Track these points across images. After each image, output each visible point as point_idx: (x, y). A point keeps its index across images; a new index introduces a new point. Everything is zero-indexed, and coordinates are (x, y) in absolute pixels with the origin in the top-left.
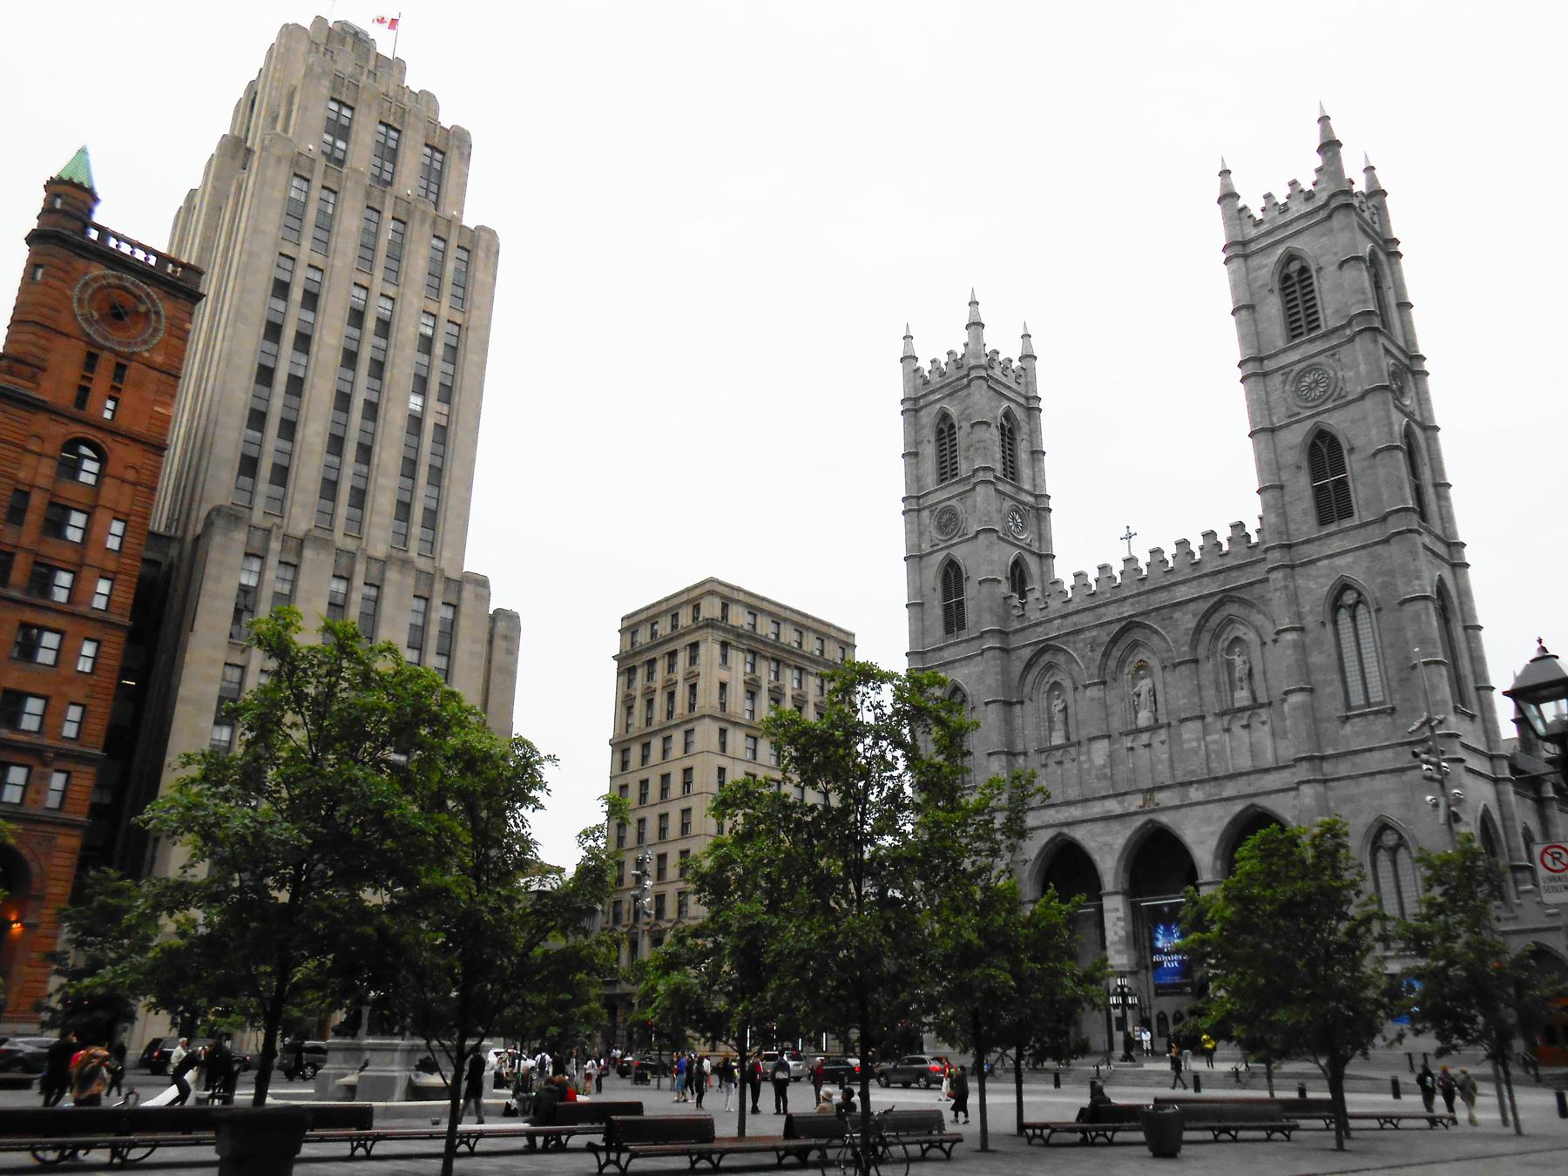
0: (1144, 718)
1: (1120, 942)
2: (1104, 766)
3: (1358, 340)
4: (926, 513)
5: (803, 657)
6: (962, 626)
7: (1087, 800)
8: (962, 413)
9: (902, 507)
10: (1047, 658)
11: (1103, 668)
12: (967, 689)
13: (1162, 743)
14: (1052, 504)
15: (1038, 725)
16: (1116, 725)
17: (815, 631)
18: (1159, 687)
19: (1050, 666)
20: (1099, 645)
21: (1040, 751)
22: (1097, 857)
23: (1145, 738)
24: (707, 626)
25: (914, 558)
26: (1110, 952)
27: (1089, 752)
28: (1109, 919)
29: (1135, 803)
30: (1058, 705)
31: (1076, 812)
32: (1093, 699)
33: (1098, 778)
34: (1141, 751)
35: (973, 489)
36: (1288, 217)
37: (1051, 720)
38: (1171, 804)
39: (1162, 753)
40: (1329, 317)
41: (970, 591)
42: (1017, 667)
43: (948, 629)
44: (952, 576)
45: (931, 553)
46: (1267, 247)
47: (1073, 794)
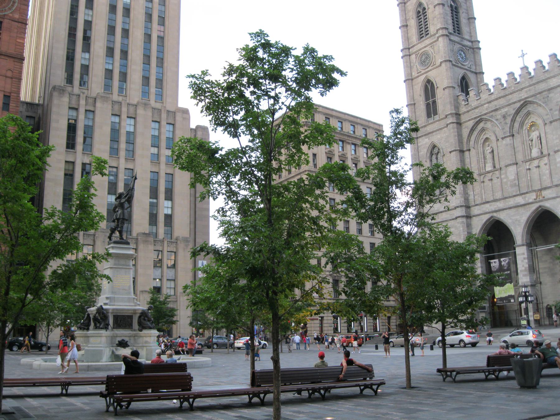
0: (535, 152)
1: (525, 270)
2: (515, 180)
4: (413, 56)
5: (356, 138)
6: (435, 113)
7: (506, 198)
9: (401, 54)
10: (481, 125)
11: (512, 127)
13: (546, 164)
14: (481, 45)
15: (478, 161)
16: (520, 157)
17: (362, 125)
18: (543, 135)
19: (483, 130)
20: (509, 115)
22: (512, 228)
23: (536, 163)
25: (409, 80)
26: (520, 275)
27: (506, 173)
28: (519, 259)
29: (532, 197)
30: (488, 150)
31: (500, 205)
32: (507, 145)
33: (512, 186)
34: (535, 170)
35: (438, 40)
37: (485, 158)
38: (551, 196)
39: (545, 170)
42: (465, 132)
43: (429, 115)
44: (429, 89)
45: (418, 77)
47: (498, 195)
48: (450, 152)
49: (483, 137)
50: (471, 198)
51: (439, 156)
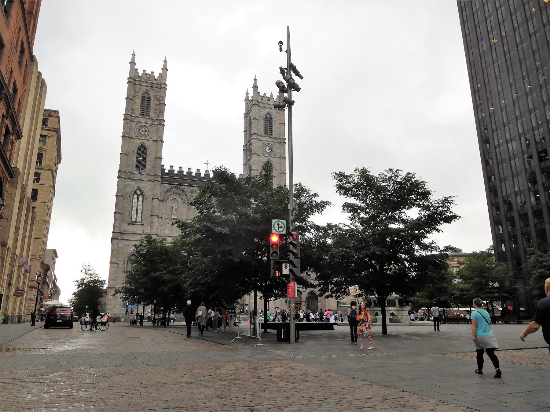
3: (282, 144)
4: (134, 123)
6: (144, 168)
8: (155, 96)
9: (123, 117)
10: (174, 190)
12: (146, 191)
19: (175, 193)
21: (168, 219)
24: (55, 131)
36: (268, 102)
40: (275, 135)
41: (149, 159)
43: (138, 167)
46: (266, 107)
48: (152, 199)
49: (174, 196)
50: (159, 230)
51: (141, 197)
